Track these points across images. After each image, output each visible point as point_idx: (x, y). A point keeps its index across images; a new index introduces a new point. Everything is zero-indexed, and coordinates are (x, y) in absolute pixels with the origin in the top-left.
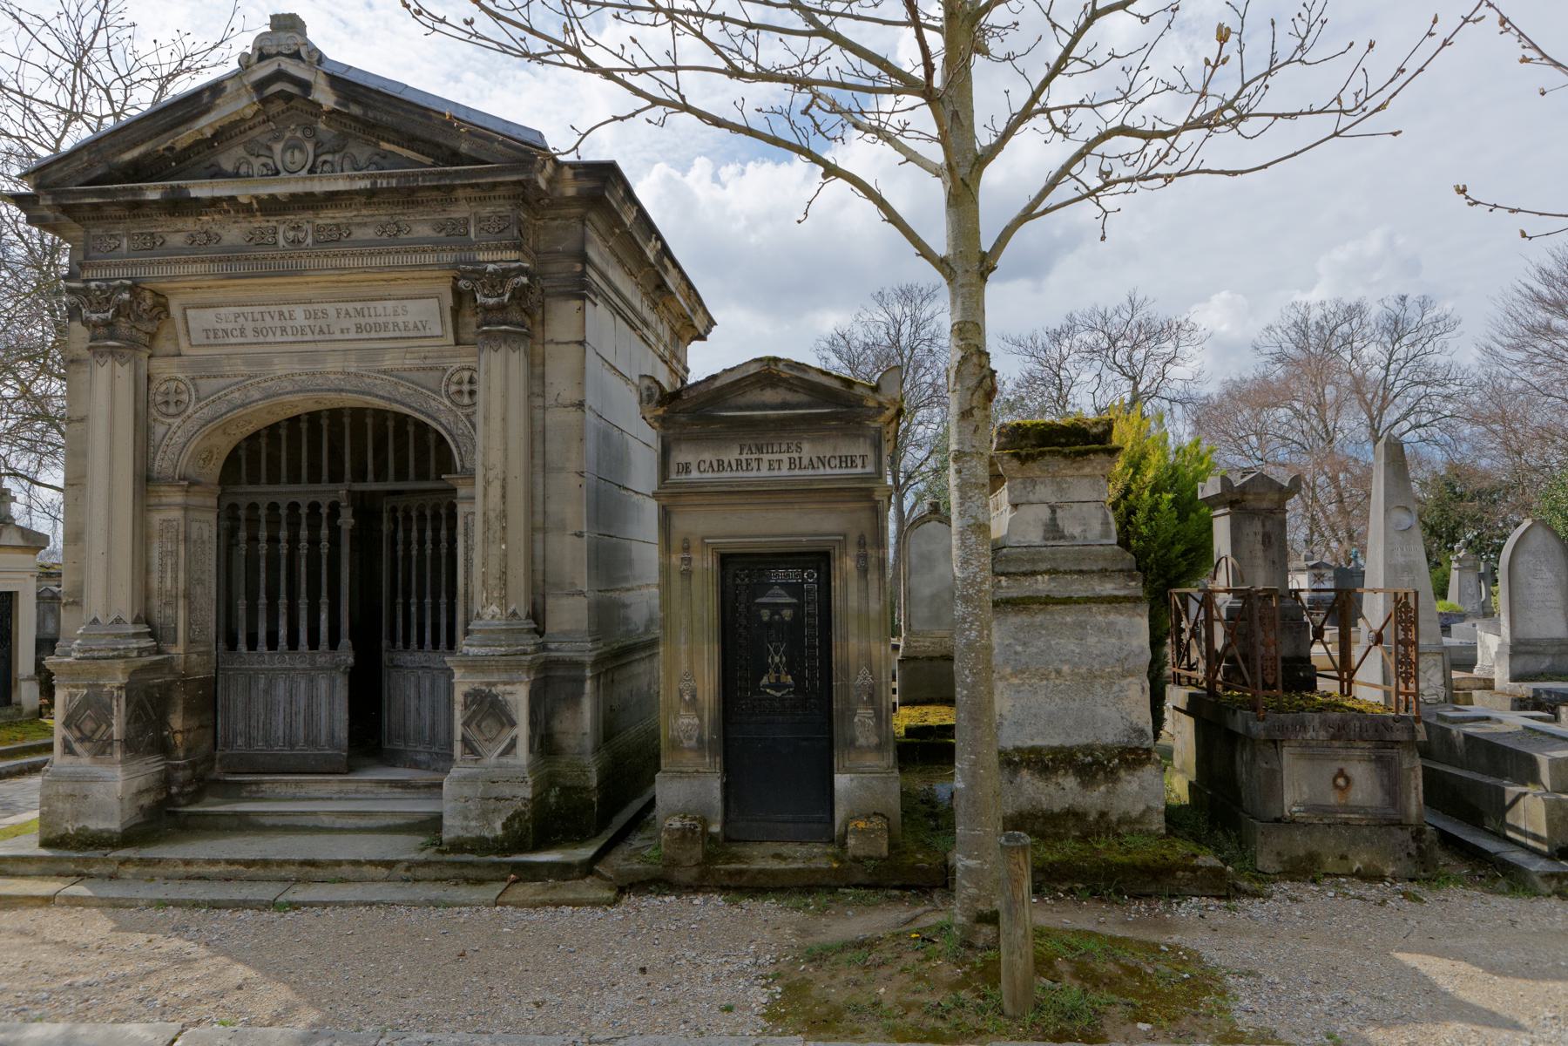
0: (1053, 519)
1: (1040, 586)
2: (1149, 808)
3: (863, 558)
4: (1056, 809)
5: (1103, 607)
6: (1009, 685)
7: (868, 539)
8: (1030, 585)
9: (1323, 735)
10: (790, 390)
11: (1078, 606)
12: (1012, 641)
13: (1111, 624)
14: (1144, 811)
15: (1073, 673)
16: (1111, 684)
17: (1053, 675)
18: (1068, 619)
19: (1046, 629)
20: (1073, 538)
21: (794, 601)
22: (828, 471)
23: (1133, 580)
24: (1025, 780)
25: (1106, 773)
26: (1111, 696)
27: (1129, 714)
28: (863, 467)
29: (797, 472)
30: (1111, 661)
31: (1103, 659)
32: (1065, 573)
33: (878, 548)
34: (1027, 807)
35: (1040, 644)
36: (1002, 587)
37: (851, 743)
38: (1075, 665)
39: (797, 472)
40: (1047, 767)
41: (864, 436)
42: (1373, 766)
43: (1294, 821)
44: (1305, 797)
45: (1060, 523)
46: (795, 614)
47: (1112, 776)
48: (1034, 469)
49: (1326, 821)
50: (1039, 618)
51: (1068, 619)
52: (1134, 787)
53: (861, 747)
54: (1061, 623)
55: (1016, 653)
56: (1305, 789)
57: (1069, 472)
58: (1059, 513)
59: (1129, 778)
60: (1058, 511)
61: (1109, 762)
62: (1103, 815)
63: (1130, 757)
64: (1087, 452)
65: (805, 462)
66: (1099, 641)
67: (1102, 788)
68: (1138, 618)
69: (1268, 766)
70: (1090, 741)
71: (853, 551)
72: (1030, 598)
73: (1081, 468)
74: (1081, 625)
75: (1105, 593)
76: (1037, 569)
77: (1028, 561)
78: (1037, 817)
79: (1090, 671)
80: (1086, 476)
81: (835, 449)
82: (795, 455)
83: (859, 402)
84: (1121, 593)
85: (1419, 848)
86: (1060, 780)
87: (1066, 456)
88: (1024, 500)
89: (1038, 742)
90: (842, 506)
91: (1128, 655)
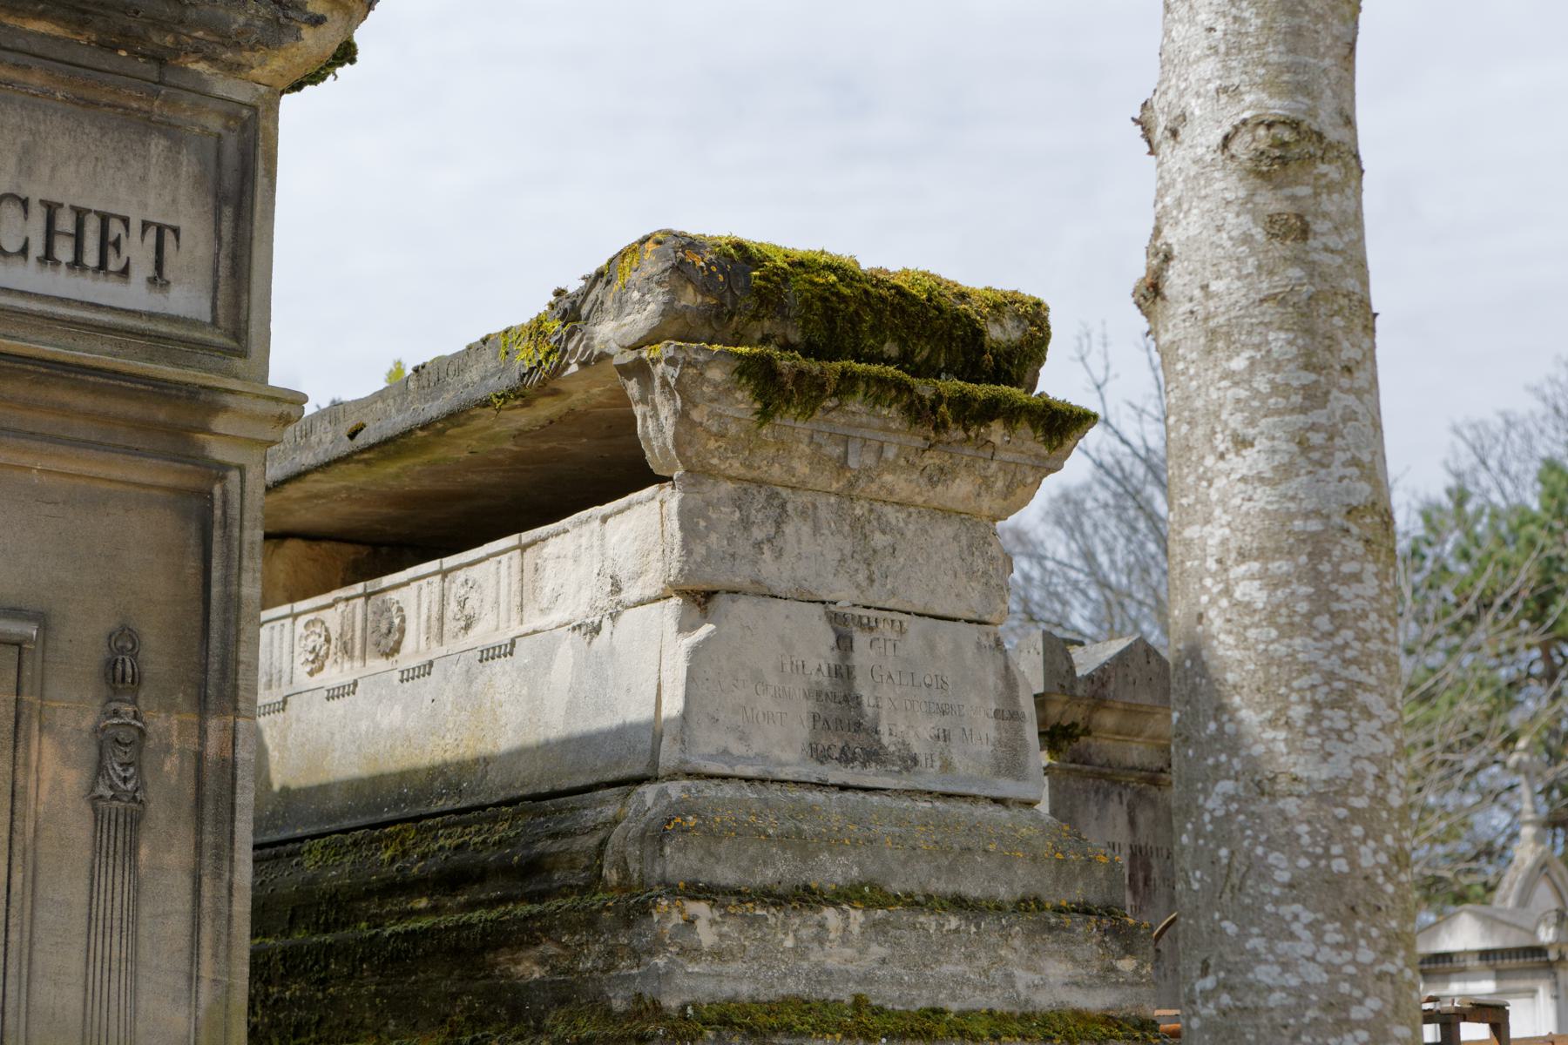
0: (843, 673)
1: (835, 957)
7: (157, 657)
8: (800, 951)
20: (910, 762)
23: (1128, 951)
28: (158, 279)
32: (913, 903)
33: (202, 706)
36: (692, 952)
41: (169, 130)
57: (901, 484)
58: (864, 652)
60: (861, 639)
72: (802, 1005)
73: (942, 475)
75: (1043, 1001)
77: (784, 839)
80: (947, 513)
81: (27, 160)
87: (920, 412)
90: (40, 463)
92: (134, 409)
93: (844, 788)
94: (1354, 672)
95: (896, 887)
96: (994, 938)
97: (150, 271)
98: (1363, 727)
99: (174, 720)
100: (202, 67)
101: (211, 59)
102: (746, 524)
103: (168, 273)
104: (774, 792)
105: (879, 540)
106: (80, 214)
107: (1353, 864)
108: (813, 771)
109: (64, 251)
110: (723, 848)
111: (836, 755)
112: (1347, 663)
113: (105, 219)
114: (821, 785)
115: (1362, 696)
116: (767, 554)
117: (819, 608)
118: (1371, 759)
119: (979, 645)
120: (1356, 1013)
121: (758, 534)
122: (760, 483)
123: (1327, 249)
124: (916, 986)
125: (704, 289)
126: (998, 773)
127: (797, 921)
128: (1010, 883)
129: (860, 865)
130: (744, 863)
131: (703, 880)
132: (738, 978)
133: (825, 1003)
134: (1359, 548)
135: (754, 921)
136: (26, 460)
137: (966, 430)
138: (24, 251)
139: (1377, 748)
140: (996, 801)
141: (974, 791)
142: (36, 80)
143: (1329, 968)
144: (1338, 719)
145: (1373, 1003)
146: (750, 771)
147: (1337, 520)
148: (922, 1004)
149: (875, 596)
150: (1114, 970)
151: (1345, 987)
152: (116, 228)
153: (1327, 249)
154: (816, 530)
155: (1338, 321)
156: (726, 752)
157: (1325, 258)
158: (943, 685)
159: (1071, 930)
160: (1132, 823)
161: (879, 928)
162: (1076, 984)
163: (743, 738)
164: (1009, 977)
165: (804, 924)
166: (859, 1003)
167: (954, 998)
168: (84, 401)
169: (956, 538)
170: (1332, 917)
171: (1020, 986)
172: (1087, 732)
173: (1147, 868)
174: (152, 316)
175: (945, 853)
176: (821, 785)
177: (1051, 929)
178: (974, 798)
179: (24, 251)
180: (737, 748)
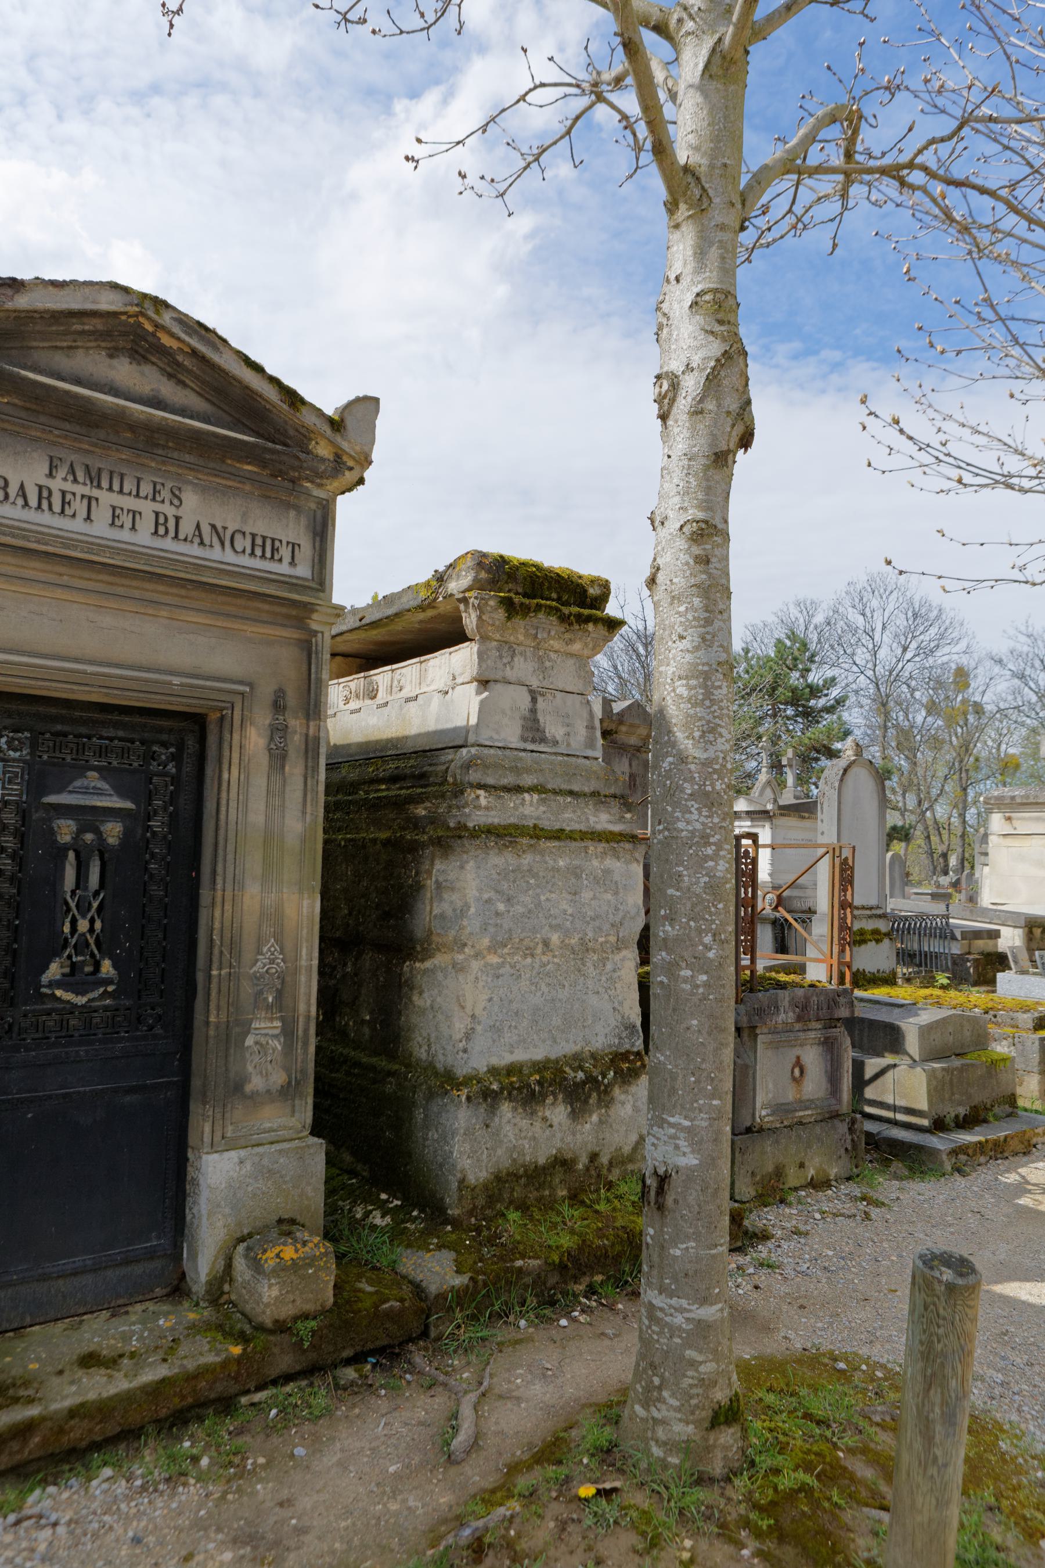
0: (533, 711)
1: (528, 810)
4: (542, 1161)
5: (602, 846)
6: (486, 965)
7: (292, 699)
8: (516, 808)
9: (791, 1017)
10: (170, 376)
11: (574, 844)
12: (492, 894)
13: (607, 872)
15: (564, 945)
16: (604, 961)
19: (535, 876)
20: (556, 743)
21: (129, 805)
22: (229, 556)
23: (629, 811)
24: (505, 1120)
27: (621, 1003)
28: (293, 563)
29: (168, 544)
30: (606, 927)
32: (555, 792)
33: (308, 717)
34: (506, 1164)
35: (527, 899)
36: (478, 807)
37: (237, 1088)
38: (567, 933)
39: (168, 544)
41: (297, 508)
42: (821, 1048)
43: (761, 1130)
46: (127, 834)
47: (605, 1097)
48: (520, 630)
49: (786, 1123)
50: (527, 859)
51: (561, 863)
53: (253, 1096)
54: (553, 868)
57: (556, 644)
58: (541, 704)
59: (623, 1097)
60: (540, 699)
61: (604, 1077)
65: (187, 528)
67: (595, 1118)
71: (263, 717)
72: (516, 827)
73: (570, 642)
74: (576, 872)
75: (599, 827)
78: (517, 1177)
80: (572, 655)
81: (245, 517)
82: (170, 511)
83: (302, 439)
84: (617, 828)
85: (853, 1140)
86: (547, 1113)
87: (564, 619)
89: (520, 1056)
90: (252, 629)
91: (624, 918)
92: (284, 610)
93: (532, 751)
94: (717, 721)
95: (549, 786)
97: (290, 560)
98: (719, 740)
99: (298, 722)
100: (308, 485)
101: (312, 482)
102: (501, 657)
103: (296, 561)
104: (508, 752)
105: (548, 664)
106: (264, 538)
107: (713, 788)
108: (522, 745)
109: (258, 552)
110: (489, 772)
112: (715, 717)
113: (273, 540)
114: (524, 750)
115: (719, 729)
116: (508, 668)
117: (525, 688)
118: (721, 751)
119: (581, 702)
120: (712, 840)
121: (505, 660)
122: (506, 642)
123: (716, 568)
125: (488, 571)
126: (586, 748)
131: (483, 782)
132: (494, 817)
134: (721, 677)
135: (500, 797)
136: (245, 628)
138: (244, 551)
139: (724, 748)
140: (585, 757)
142: (248, 487)
143: (703, 824)
144: (711, 737)
145: (717, 837)
146: (500, 745)
147: (714, 666)
148: (557, 827)
149: (545, 684)
151: (708, 831)
152: (277, 544)
153: (716, 568)
154: (525, 659)
155: (718, 595)
156: (491, 738)
157: (715, 571)
158: (568, 716)
160: (630, 765)
161: (543, 801)
163: (498, 733)
164: (587, 819)
166: (535, 826)
168: (266, 607)
170: (705, 806)
171: (591, 822)
172: (616, 732)
173: (635, 781)
174: (290, 576)
176: (524, 750)
177: (602, 803)
178: (578, 756)
179: (244, 551)
180: (496, 737)
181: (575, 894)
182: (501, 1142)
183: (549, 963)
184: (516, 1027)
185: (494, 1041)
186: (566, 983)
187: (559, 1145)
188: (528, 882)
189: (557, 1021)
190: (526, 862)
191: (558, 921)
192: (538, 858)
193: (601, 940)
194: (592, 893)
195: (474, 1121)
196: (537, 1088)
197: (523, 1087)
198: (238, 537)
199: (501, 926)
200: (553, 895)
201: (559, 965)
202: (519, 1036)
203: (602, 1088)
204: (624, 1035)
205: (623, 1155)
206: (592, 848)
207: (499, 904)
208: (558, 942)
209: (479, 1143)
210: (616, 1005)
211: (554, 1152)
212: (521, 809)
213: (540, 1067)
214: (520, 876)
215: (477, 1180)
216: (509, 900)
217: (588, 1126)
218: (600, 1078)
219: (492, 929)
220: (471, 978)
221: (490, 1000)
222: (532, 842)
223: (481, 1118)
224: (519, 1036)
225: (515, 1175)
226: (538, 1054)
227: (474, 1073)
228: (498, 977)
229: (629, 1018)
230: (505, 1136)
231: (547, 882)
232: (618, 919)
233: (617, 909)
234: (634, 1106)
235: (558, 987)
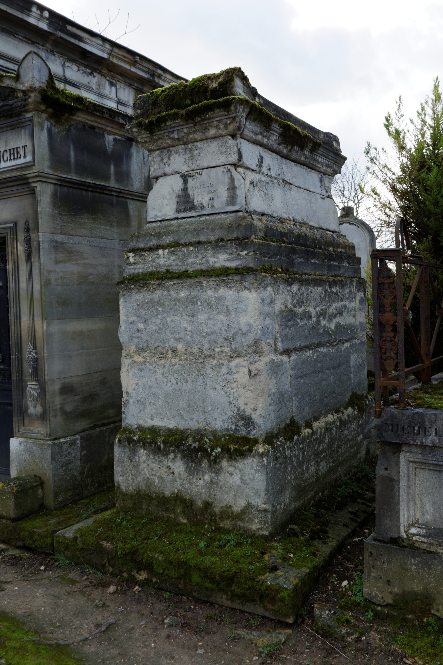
0: (185, 189)
1: (162, 261)
2: (249, 506)
3: (28, 241)
4: (167, 493)
5: (212, 281)
6: (134, 362)
8: (153, 261)
12: (135, 318)
13: (220, 299)
14: (246, 508)
17: (170, 355)
18: (182, 295)
19: (162, 305)
25: (209, 461)
26: (220, 379)
30: (221, 340)
31: (212, 337)
32: (186, 245)
35: (158, 321)
36: (129, 264)
40: (159, 448)
44: (429, 517)
45: (190, 192)
50: (158, 294)
52: (236, 480)
55: (138, 330)
56: (428, 507)
59: (231, 469)
60: (190, 180)
61: (212, 450)
62: (207, 505)
63: (232, 447)
64: (209, 108)
66: (209, 319)
68: (246, 292)
69: (386, 473)
70: (201, 425)
73: (206, 129)
75: (217, 265)
76: (162, 243)
79: (201, 350)
86: (170, 464)
88: (160, 172)
89: (157, 422)
91: (235, 334)
95: (182, 242)
96: (203, 251)
102: (162, 160)
104: (164, 223)
110: (141, 239)
111: (183, 210)
113: (17, 148)
116: (167, 166)
117: (179, 175)
124: (181, 266)
126: (228, 205)
127: (152, 254)
128: (214, 236)
129: (173, 238)
130: (145, 242)
132: (139, 269)
133: (158, 272)
135: (142, 255)
137: (201, 117)
141: (217, 212)
146: (160, 219)
148: (183, 270)
150: (240, 255)
159: (225, 246)
162: (228, 260)
164: (207, 261)
165: (154, 254)
166: (167, 271)
167: (192, 267)
169: (218, 145)
171: (211, 263)
175: (195, 231)
176: (177, 219)
181: (193, 316)
182: (140, 473)
183: (176, 364)
184: (154, 404)
185: (141, 410)
186: (188, 379)
187: (179, 487)
188: (157, 309)
189: (183, 404)
190: (157, 296)
191: (181, 336)
192: (165, 293)
193: (217, 350)
194: (206, 316)
195: (123, 455)
196: (162, 446)
197: (153, 443)
198: (5, 153)
199: (141, 338)
200: (176, 318)
201: (184, 366)
202: (157, 410)
203: (212, 458)
204: (240, 423)
205: (232, 513)
206: (205, 282)
207: (139, 324)
208: (183, 350)
209: (127, 470)
210: (231, 400)
211: (176, 491)
212: (157, 261)
213: (171, 432)
214: (151, 306)
215: (126, 491)
216: (145, 321)
217: (201, 482)
218: (209, 450)
219: (136, 340)
220: (126, 368)
221: (137, 384)
222: (158, 282)
223: (127, 455)
224: (157, 410)
225: (150, 496)
226: (171, 424)
227: (129, 427)
228: (141, 371)
229: (243, 411)
230: (143, 470)
231: (171, 309)
232: (230, 335)
233: (229, 326)
234: (241, 478)
235: (183, 381)
